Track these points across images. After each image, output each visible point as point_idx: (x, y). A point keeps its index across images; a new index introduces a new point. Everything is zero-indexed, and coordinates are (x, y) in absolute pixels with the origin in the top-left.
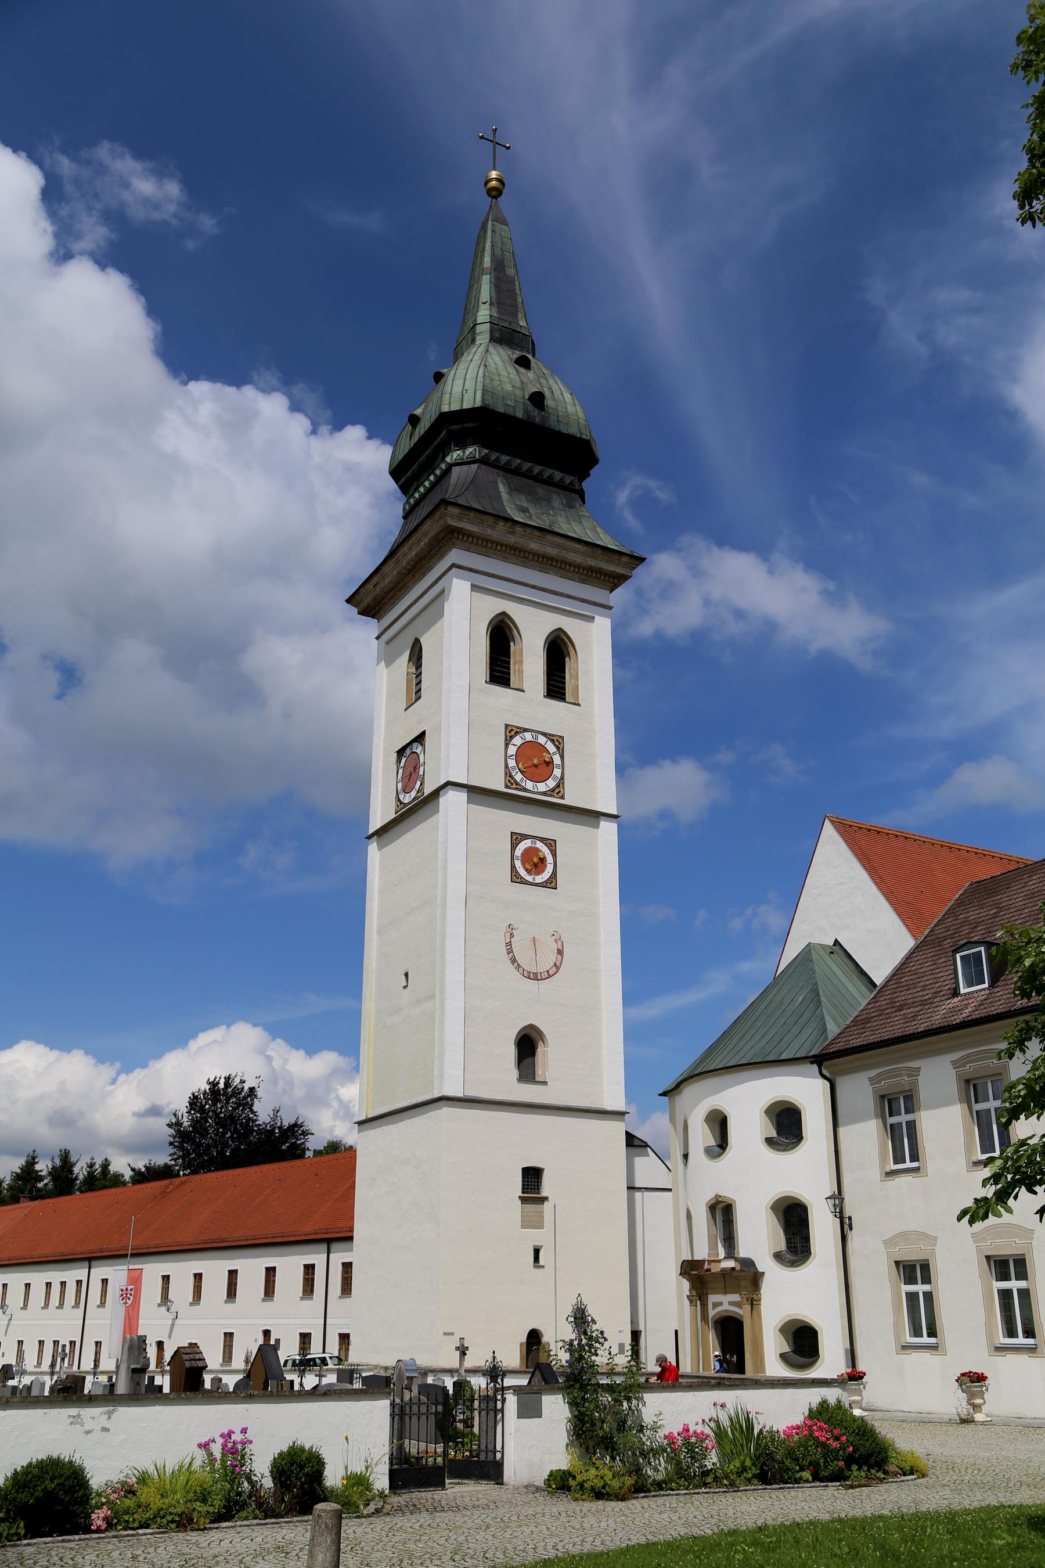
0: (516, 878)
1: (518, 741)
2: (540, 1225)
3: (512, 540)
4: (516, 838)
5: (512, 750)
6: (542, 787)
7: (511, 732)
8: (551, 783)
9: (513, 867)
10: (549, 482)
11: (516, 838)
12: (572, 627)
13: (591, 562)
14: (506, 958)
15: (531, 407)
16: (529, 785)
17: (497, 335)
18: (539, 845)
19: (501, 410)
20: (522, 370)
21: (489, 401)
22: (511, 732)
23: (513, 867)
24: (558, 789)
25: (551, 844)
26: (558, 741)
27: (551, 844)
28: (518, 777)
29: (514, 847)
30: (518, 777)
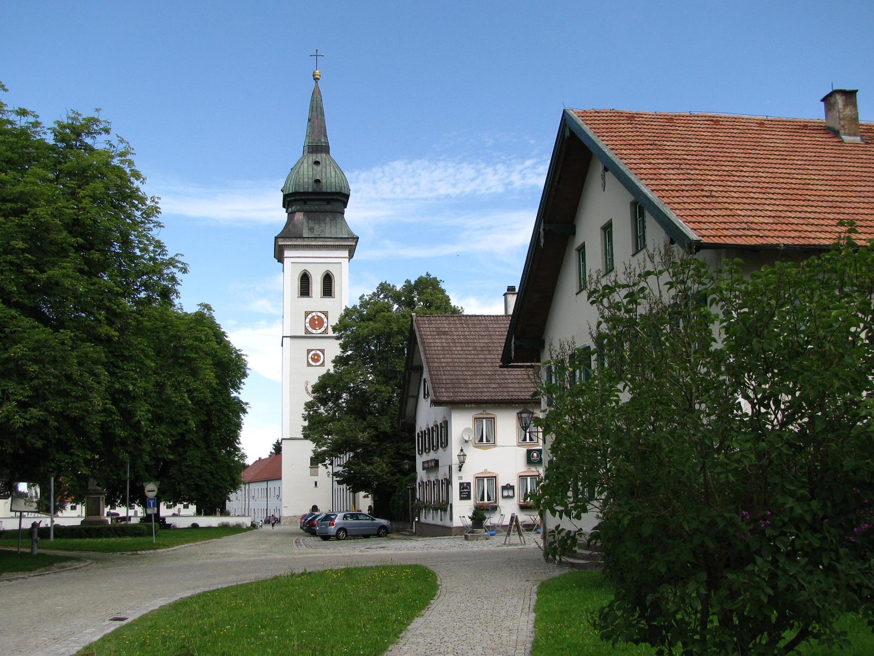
0: (309, 365)
1: (310, 316)
3: (304, 243)
4: (309, 351)
5: (308, 320)
7: (307, 314)
8: (323, 329)
10: (326, 212)
11: (309, 351)
13: (337, 243)
14: (305, 392)
15: (315, 185)
16: (314, 331)
19: (302, 191)
20: (315, 167)
21: (297, 190)
22: (307, 314)
24: (326, 331)
25: (323, 351)
26: (326, 313)
27: (323, 351)
28: (310, 329)
29: (308, 354)
30: (310, 329)
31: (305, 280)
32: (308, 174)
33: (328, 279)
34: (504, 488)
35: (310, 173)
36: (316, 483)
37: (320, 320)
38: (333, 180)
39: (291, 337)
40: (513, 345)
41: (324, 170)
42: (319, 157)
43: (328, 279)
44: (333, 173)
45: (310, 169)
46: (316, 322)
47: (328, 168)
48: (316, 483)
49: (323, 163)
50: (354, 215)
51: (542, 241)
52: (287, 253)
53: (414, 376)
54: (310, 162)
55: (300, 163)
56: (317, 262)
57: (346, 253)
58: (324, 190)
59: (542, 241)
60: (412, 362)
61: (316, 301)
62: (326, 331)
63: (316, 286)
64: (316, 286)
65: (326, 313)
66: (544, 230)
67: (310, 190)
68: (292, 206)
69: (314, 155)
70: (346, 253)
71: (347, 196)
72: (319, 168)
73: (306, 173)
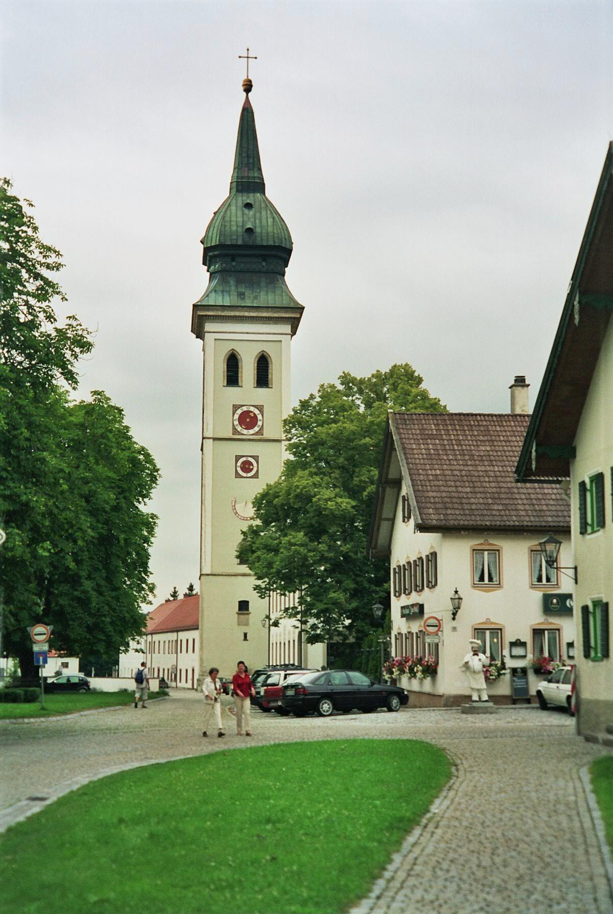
0: (238, 475)
2: (247, 624)
4: (238, 458)
5: (236, 417)
6: (252, 432)
7: (236, 407)
9: (236, 470)
10: (260, 272)
11: (238, 458)
12: (270, 350)
15: (246, 236)
16: (245, 432)
17: (240, 188)
18: (250, 459)
20: (246, 211)
22: (236, 407)
23: (236, 470)
24: (260, 432)
25: (256, 458)
26: (260, 408)
27: (256, 458)
30: (239, 428)
31: (233, 363)
32: (239, 219)
33: (263, 363)
34: (512, 644)
35: (240, 219)
36: (245, 635)
37: (245, 414)
38: (270, 229)
39: (215, 439)
40: (534, 454)
41: (258, 215)
42: (250, 198)
43: (263, 363)
44: (270, 220)
45: (240, 214)
46: (248, 420)
47: (264, 213)
48: (245, 635)
49: (256, 206)
50: (298, 278)
51: (577, 317)
52: (208, 327)
53: (389, 491)
54: (240, 204)
55: (226, 205)
56: (249, 338)
57: (287, 328)
58: (258, 242)
59: (577, 317)
60: (387, 474)
61: (248, 392)
62: (260, 432)
63: (248, 371)
64: (248, 371)
65: (260, 408)
66: (579, 302)
67: (240, 243)
68: (216, 263)
69: (245, 194)
70: (287, 328)
71: (289, 252)
72: (251, 213)
73: (234, 219)
